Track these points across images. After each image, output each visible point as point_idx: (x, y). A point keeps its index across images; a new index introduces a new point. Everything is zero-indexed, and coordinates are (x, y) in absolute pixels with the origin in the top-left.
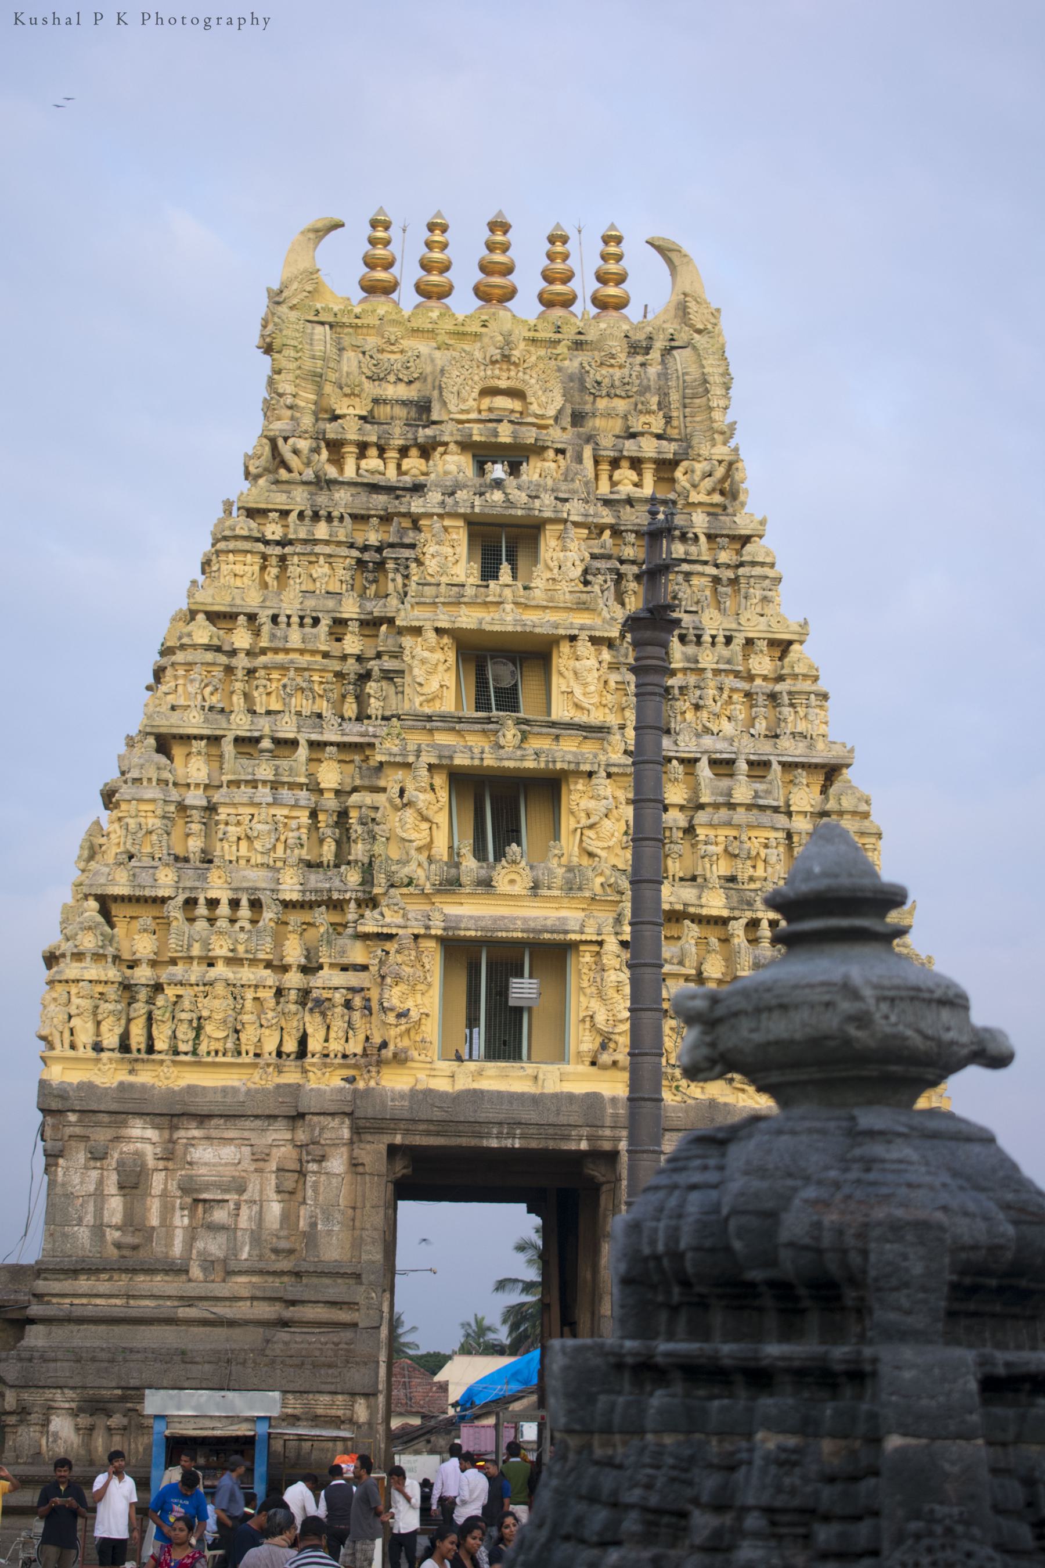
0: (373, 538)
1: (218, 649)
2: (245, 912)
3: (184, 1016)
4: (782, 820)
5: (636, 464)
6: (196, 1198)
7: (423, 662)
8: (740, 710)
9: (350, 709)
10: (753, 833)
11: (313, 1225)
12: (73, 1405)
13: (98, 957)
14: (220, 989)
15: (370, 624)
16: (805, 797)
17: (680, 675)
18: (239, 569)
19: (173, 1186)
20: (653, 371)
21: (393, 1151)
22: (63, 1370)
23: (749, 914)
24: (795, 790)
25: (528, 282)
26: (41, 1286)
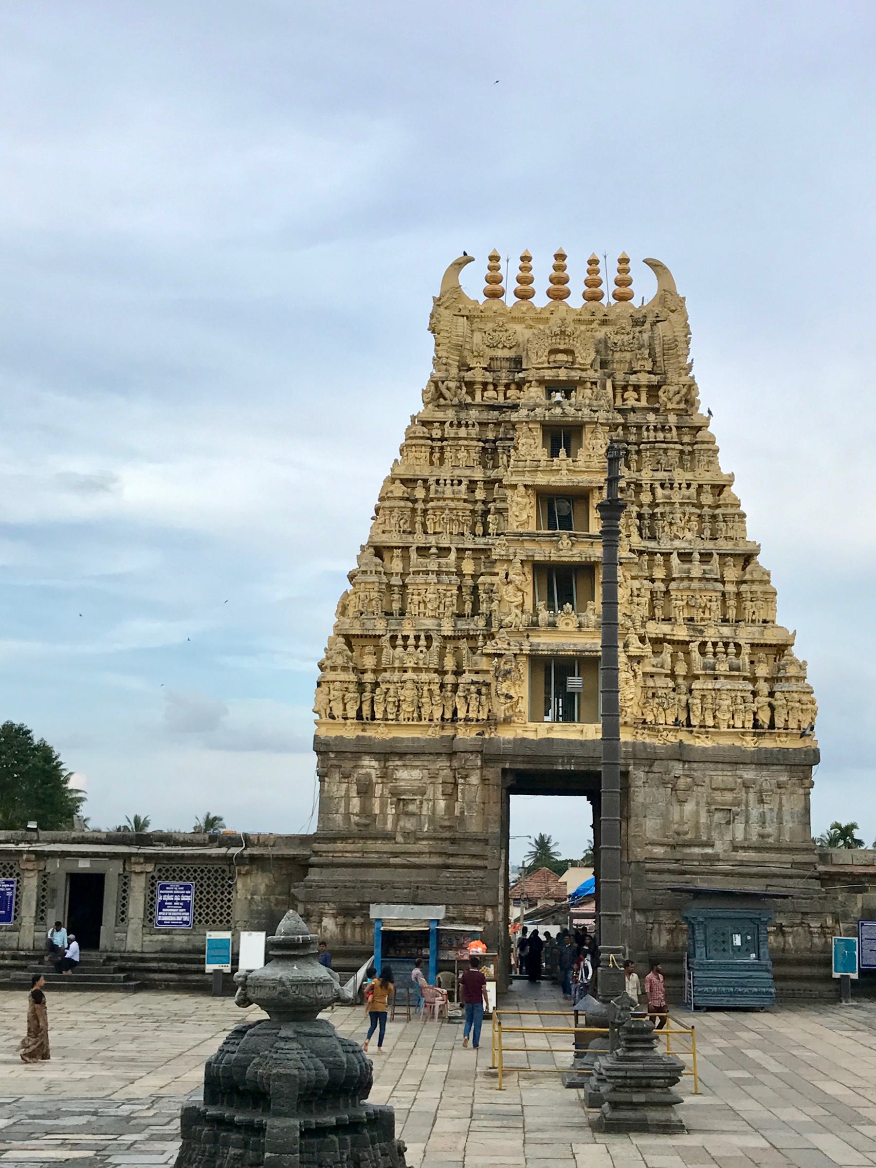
0: (491, 436)
1: (407, 499)
2: (423, 642)
3: (390, 699)
4: (719, 586)
5: (637, 388)
6: (399, 798)
7: (518, 504)
8: (694, 525)
9: (479, 530)
10: (703, 594)
11: (462, 813)
12: (334, 911)
13: (345, 669)
14: (409, 685)
15: (490, 483)
16: (732, 573)
17: (661, 506)
18: (418, 455)
19: (386, 792)
20: (646, 336)
21: (504, 771)
22: (328, 892)
23: (701, 639)
24: (726, 569)
25: (577, 287)
26: (316, 846)
